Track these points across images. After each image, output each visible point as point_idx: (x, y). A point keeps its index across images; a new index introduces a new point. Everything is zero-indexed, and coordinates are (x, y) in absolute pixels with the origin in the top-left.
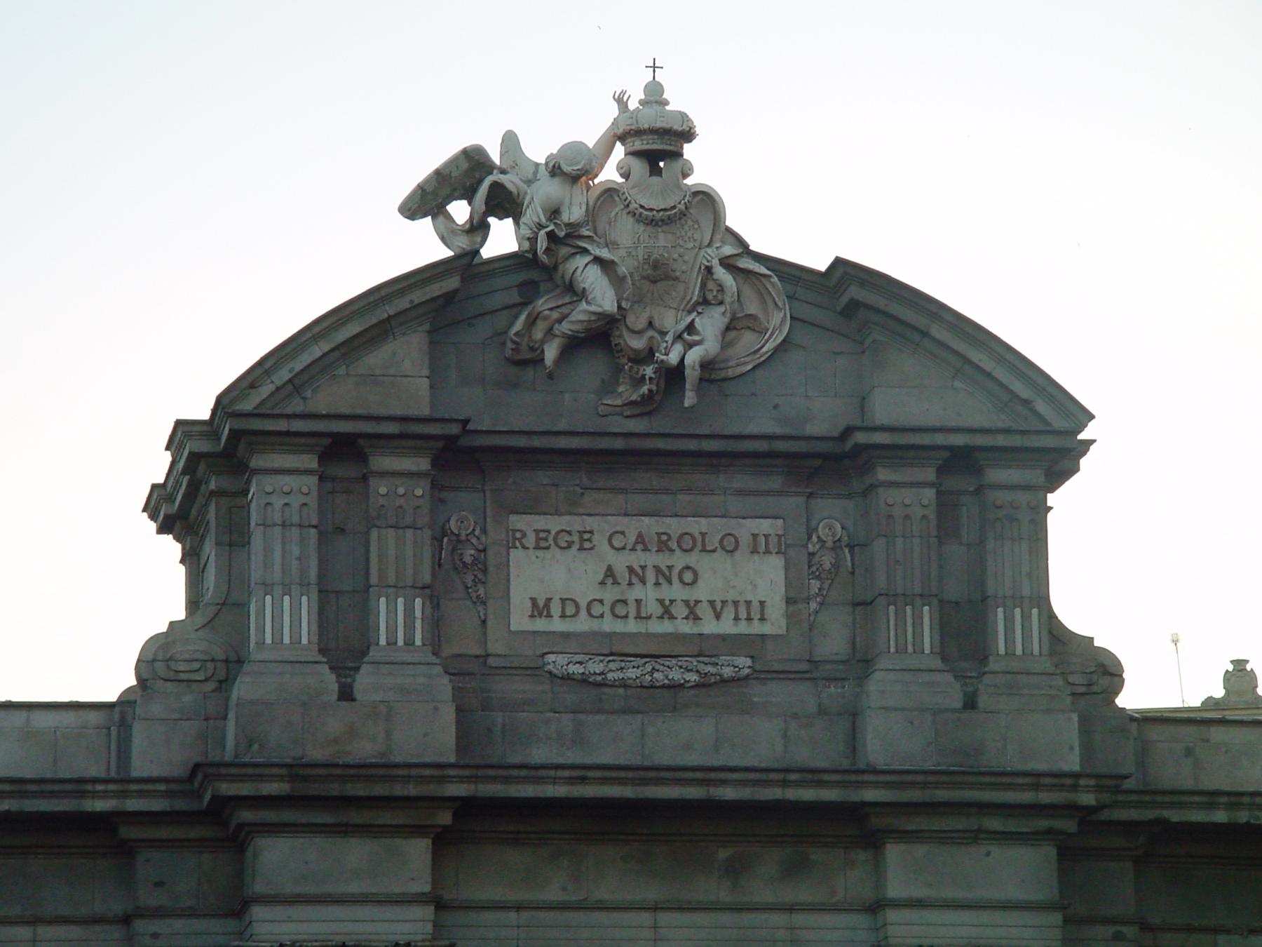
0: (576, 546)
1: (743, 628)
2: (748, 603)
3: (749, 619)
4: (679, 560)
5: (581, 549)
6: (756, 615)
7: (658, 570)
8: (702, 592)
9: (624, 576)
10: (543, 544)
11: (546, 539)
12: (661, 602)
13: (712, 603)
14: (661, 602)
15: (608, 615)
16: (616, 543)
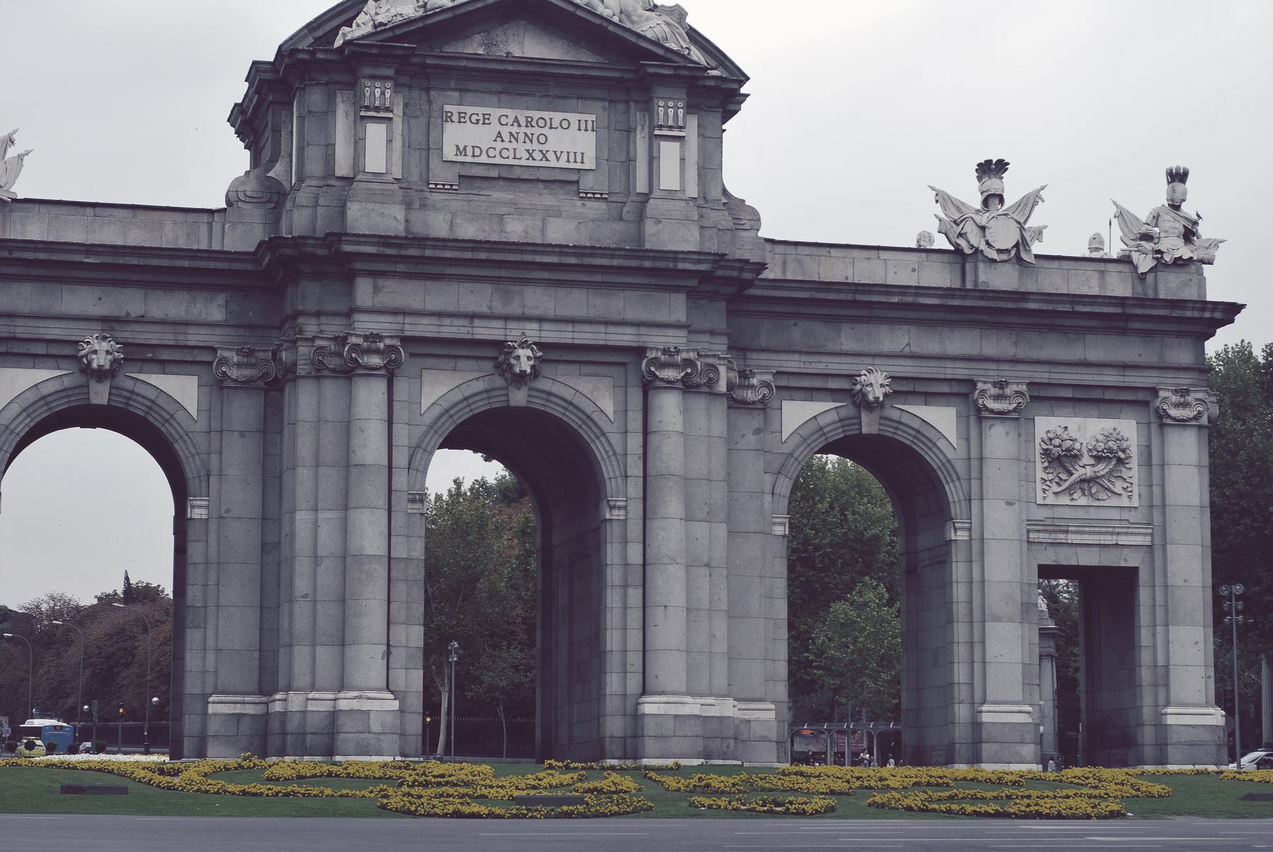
0: (481, 122)
1: (572, 166)
2: (575, 153)
3: (575, 162)
4: (537, 131)
5: (484, 123)
6: (579, 159)
7: (526, 135)
8: (548, 147)
9: (506, 137)
10: (462, 120)
11: (464, 118)
12: (528, 151)
13: (555, 152)
14: (528, 151)
15: (498, 156)
16: (504, 120)
